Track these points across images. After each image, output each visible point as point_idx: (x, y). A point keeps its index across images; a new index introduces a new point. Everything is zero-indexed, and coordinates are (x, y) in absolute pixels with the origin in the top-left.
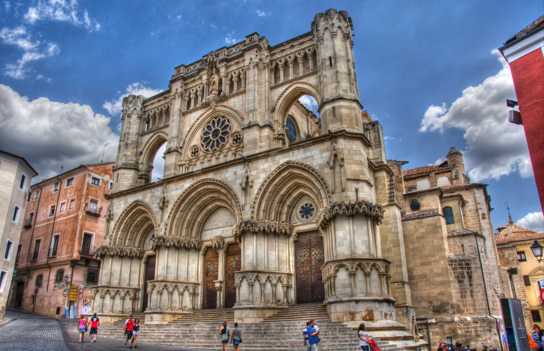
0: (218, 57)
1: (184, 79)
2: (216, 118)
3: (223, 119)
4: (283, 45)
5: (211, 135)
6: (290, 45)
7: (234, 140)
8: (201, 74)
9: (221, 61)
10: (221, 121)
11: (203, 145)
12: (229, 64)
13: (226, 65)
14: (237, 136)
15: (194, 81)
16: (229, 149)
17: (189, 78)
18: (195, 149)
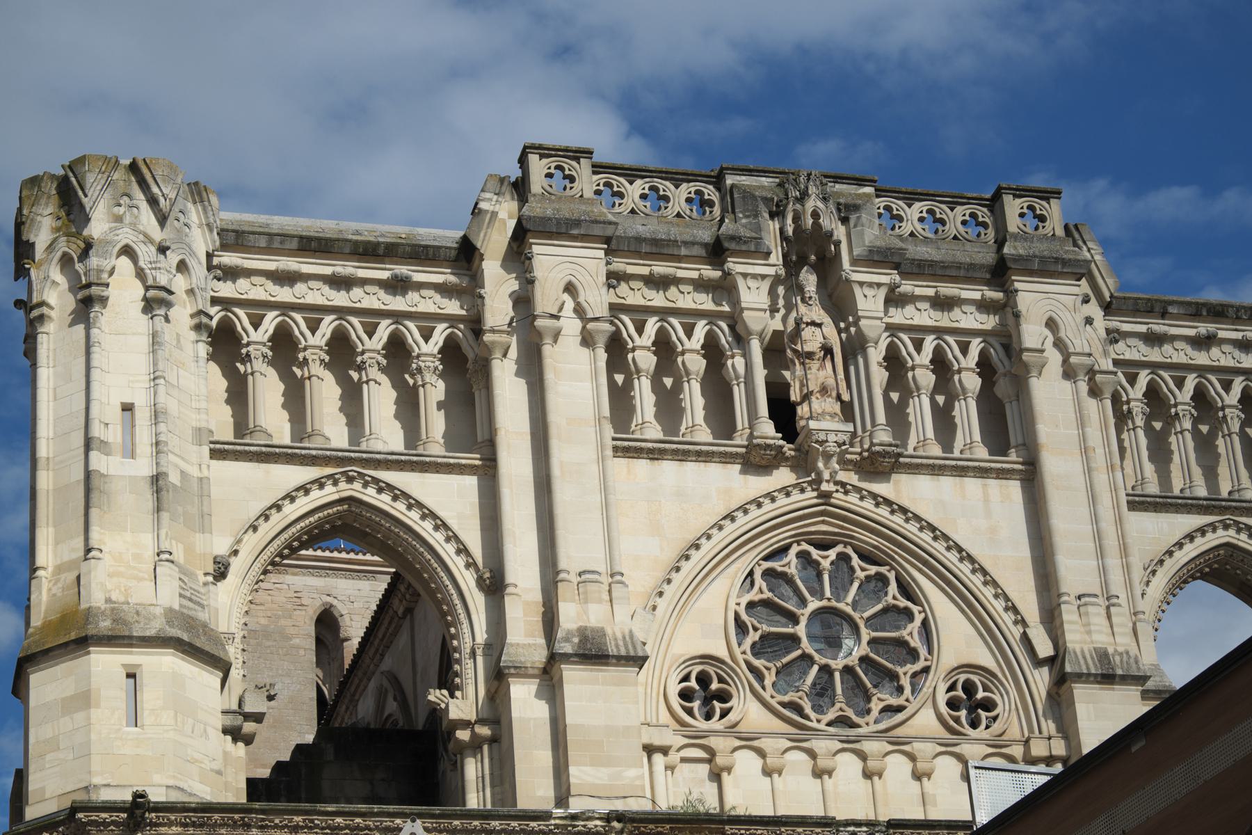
0: (845, 221)
1: (613, 246)
2: (824, 546)
3: (873, 570)
4: (1164, 315)
5: (801, 630)
6: (1203, 328)
7: (953, 704)
8: (736, 265)
9: (877, 258)
10: (861, 574)
11: (760, 677)
12: (907, 287)
13: (892, 288)
14: (969, 688)
15: (661, 283)
16: (947, 749)
17: (638, 254)
18: (703, 680)
